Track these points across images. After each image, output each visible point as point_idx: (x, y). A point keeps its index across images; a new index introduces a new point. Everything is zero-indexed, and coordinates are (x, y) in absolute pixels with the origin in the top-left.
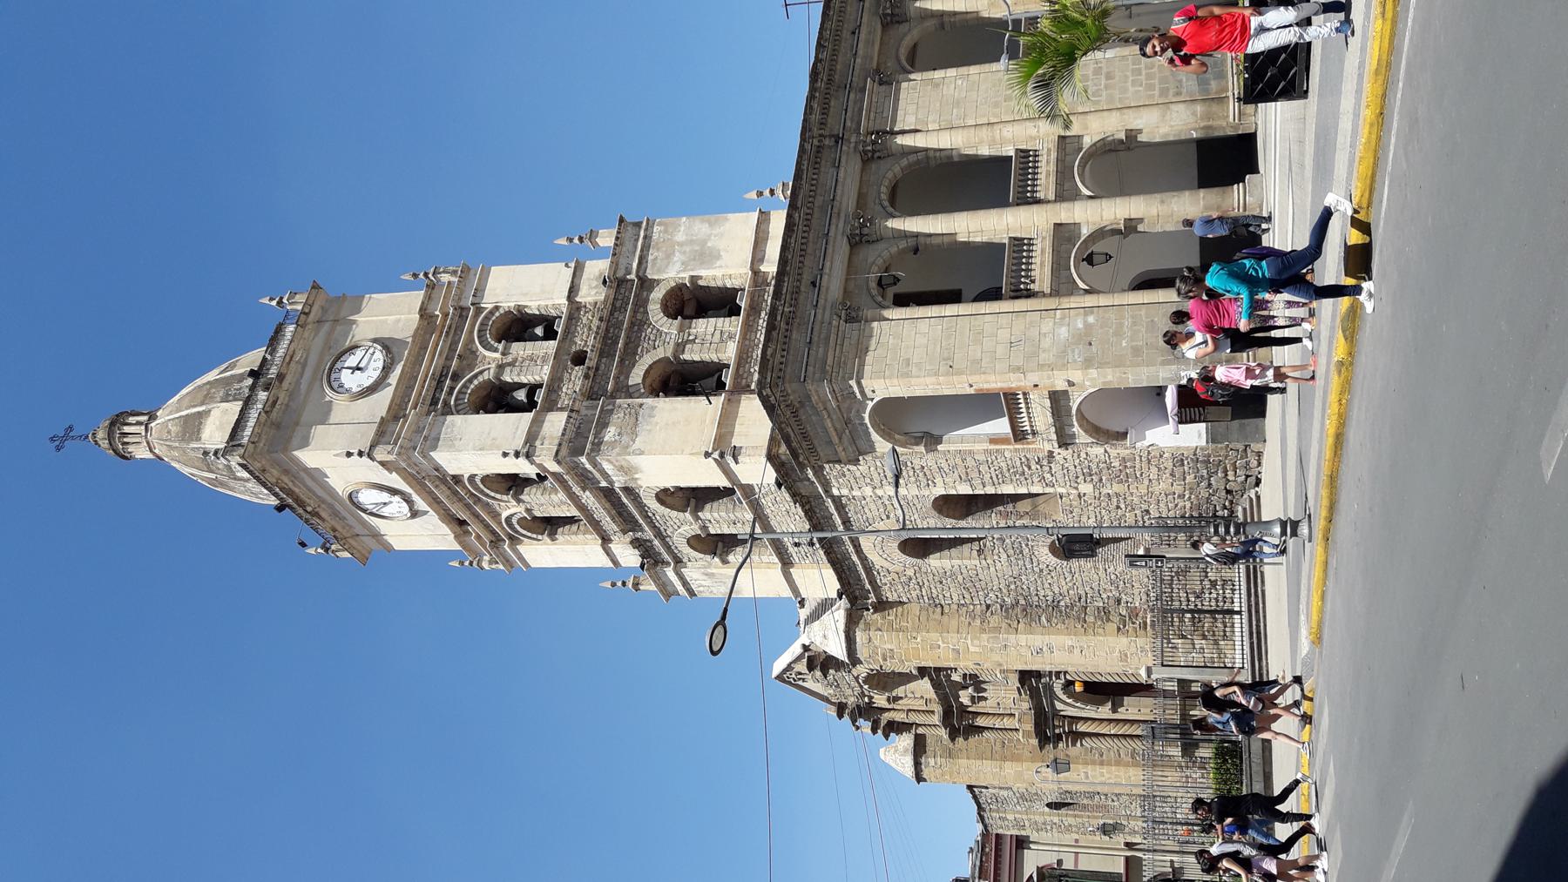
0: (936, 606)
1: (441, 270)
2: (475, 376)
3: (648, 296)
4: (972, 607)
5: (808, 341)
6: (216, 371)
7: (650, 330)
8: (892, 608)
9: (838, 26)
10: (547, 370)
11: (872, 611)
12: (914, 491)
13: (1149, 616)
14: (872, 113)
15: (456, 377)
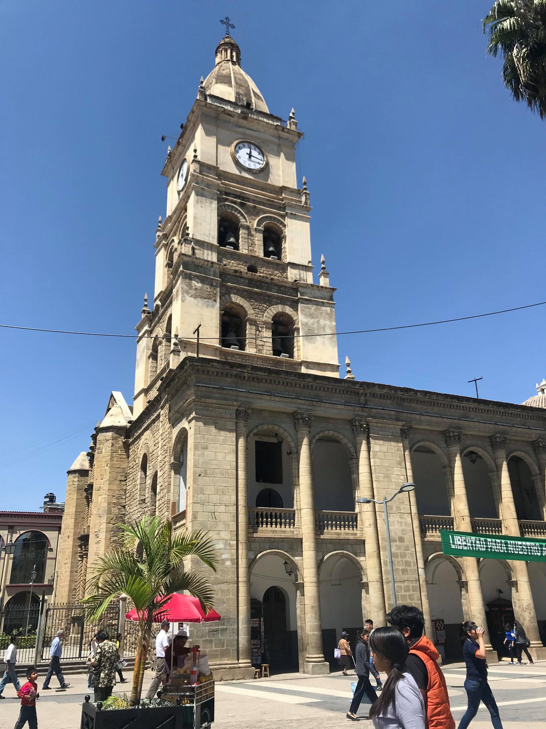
0: (126, 477)
1: (307, 197)
2: (242, 215)
3: (287, 305)
4: (124, 497)
5: (224, 388)
6: (257, 91)
7: (265, 306)
8: (126, 452)
9: (441, 404)
10: (245, 252)
11: (124, 441)
12: (160, 459)
13: (114, 599)
14: (381, 425)
15: (242, 205)
